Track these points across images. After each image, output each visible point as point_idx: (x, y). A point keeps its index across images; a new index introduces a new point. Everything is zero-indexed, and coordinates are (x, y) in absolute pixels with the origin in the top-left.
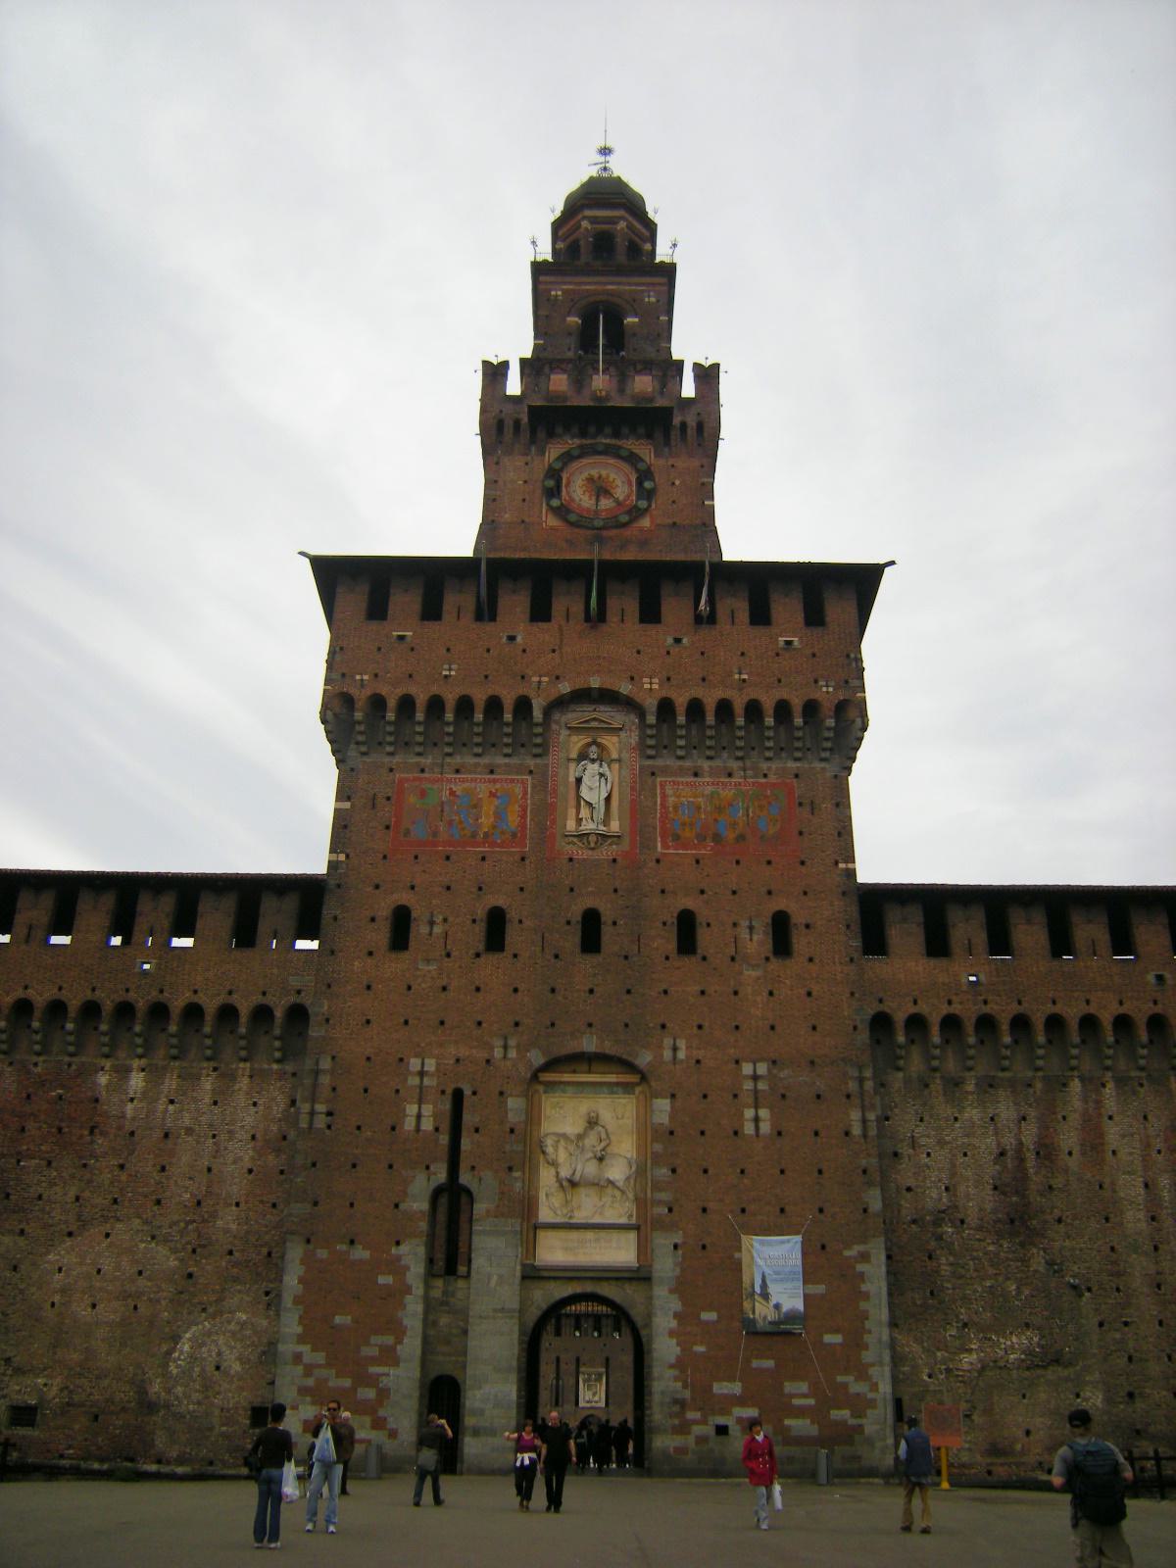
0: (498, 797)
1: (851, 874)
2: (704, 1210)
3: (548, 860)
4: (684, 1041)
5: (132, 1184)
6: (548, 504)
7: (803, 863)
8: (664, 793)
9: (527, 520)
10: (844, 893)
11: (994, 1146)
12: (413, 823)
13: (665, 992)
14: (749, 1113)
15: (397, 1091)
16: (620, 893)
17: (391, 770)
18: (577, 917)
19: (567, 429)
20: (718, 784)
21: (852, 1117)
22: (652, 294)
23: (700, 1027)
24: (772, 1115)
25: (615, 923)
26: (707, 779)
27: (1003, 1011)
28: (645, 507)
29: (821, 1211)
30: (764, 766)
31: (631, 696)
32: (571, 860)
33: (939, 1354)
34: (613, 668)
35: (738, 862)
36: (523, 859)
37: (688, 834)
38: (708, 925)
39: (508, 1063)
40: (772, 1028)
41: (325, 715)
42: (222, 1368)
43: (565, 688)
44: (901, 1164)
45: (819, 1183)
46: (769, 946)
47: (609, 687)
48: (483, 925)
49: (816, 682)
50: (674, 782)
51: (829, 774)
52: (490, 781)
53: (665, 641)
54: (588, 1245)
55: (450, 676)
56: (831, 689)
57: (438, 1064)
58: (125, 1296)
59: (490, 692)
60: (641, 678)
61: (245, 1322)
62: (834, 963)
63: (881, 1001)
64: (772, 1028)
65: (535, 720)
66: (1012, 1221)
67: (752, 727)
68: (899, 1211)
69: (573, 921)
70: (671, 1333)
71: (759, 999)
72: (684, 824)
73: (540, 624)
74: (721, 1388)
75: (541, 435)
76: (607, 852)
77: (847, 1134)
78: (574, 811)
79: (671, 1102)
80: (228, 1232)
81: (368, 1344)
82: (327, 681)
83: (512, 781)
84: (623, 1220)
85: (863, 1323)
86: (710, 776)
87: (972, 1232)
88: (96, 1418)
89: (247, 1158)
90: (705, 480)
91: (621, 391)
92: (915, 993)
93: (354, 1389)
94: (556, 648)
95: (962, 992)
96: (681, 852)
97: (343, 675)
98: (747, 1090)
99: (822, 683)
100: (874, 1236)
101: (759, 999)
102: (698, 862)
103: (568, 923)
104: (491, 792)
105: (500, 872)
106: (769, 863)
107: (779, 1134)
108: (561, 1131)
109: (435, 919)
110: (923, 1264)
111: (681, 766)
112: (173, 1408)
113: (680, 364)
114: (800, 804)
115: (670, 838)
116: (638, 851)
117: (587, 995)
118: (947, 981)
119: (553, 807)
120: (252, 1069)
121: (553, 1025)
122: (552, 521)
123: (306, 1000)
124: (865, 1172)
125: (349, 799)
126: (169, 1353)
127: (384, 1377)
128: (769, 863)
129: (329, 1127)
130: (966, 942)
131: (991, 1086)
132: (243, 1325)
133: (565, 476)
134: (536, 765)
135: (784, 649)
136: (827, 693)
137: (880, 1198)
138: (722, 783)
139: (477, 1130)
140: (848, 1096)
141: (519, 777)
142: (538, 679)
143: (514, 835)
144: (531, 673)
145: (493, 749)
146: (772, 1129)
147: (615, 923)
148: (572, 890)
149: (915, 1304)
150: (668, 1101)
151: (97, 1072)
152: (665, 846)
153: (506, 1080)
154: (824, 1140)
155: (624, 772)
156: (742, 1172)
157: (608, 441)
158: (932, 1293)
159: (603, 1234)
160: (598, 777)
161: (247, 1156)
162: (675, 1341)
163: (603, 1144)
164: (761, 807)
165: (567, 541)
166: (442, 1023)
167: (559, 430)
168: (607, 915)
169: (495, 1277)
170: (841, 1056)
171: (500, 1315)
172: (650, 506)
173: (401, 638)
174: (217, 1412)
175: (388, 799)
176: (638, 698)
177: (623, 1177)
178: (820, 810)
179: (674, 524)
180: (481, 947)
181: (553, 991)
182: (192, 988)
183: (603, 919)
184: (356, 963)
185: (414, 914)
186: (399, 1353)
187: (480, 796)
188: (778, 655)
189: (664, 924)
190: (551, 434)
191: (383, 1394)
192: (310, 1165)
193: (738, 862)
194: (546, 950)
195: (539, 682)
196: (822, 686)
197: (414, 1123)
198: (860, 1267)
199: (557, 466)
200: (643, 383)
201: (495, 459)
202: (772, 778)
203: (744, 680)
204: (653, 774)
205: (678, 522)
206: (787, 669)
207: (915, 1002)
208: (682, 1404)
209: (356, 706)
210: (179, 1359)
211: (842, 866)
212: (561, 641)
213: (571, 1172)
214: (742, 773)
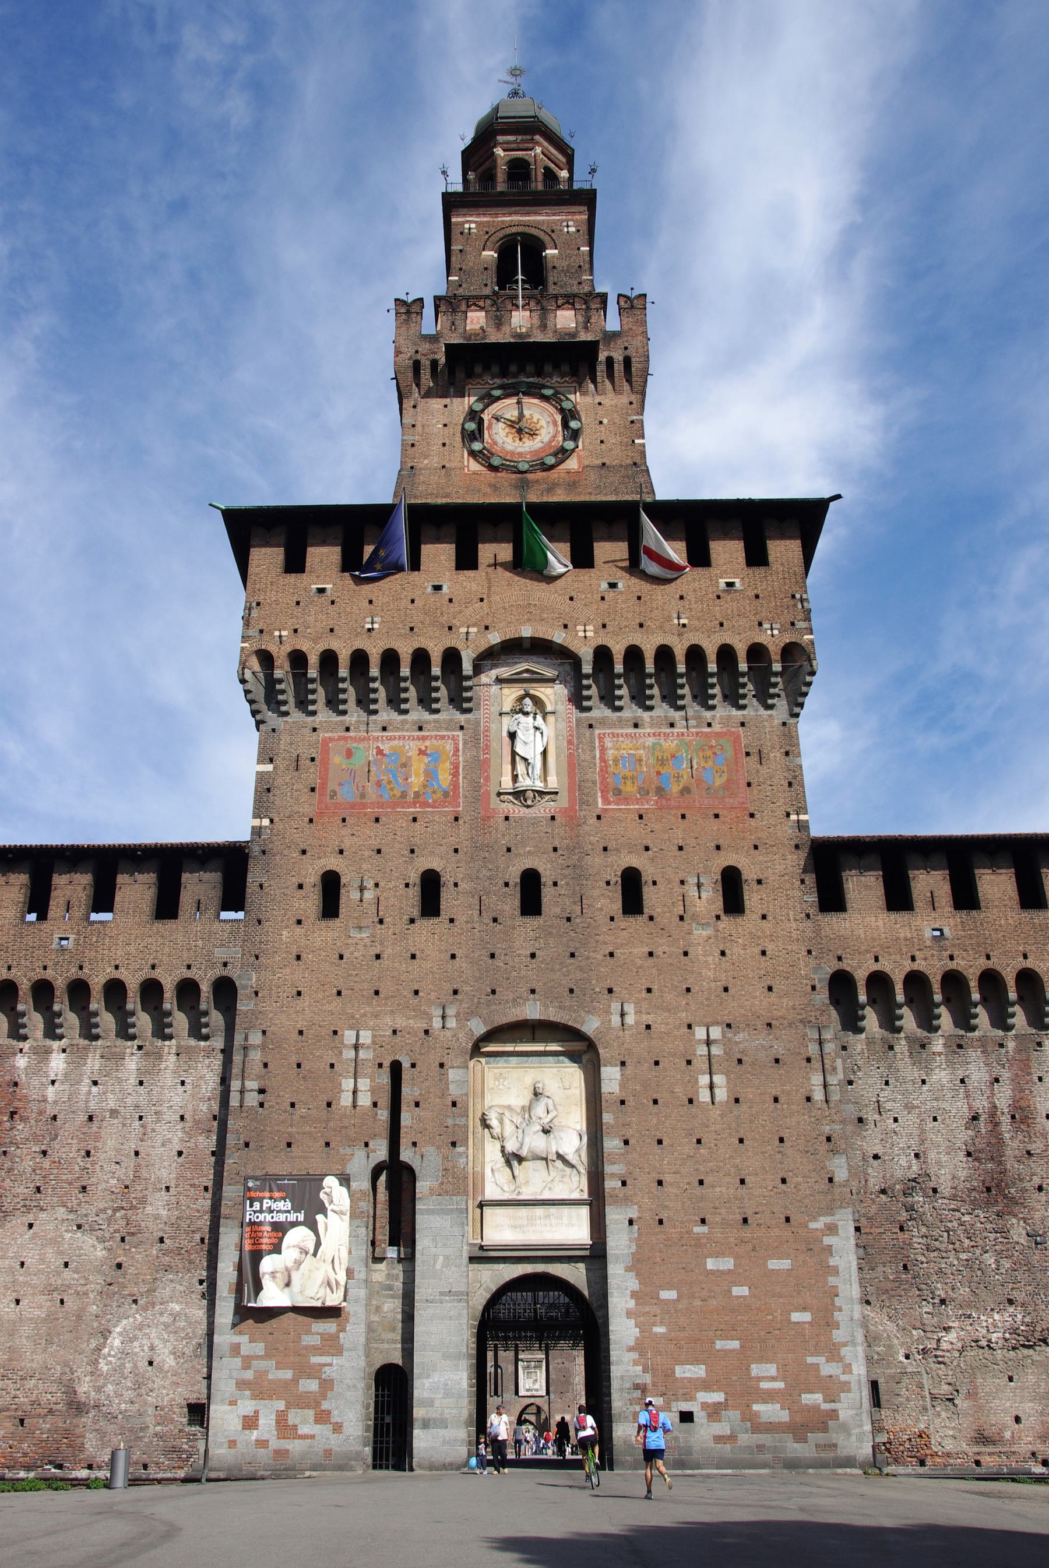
1: (802, 826)
2: (660, 1183)
3: (484, 820)
4: (632, 1005)
5: (55, 1171)
7: (752, 815)
8: (603, 746)
9: (447, 465)
10: (797, 847)
11: (966, 1110)
12: (340, 784)
13: (611, 955)
14: (704, 1080)
15: (332, 1066)
16: (560, 852)
17: (315, 730)
18: (515, 879)
19: (487, 368)
20: (659, 735)
21: (813, 1082)
22: (571, 223)
23: (649, 990)
24: (728, 1083)
25: (555, 884)
26: (648, 730)
27: (971, 966)
28: (572, 447)
29: (784, 1181)
30: (708, 715)
31: (565, 645)
32: (507, 818)
33: (914, 1332)
34: (545, 616)
35: (683, 816)
36: (456, 819)
37: (630, 788)
38: (654, 883)
39: (448, 1034)
40: (726, 990)
41: (243, 674)
42: (155, 1364)
43: (495, 638)
44: (867, 1130)
45: (779, 1152)
46: (720, 903)
47: (541, 636)
48: (418, 889)
49: (760, 624)
50: (613, 734)
51: (777, 722)
52: (418, 738)
53: (599, 586)
54: (538, 1221)
55: (373, 629)
56: (776, 632)
57: (374, 1036)
58: (50, 1290)
59: (416, 646)
60: (576, 626)
61: (178, 1314)
62: (789, 920)
63: (840, 959)
64: (726, 990)
65: (465, 673)
66: (989, 1190)
67: (694, 674)
68: (866, 1181)
69: (511, 883)
70: (629, 1314)
71: (710, 959)
72: (625, 778)
73: (465, 572)
74: (687, 1371)
75: (460, 375)
76: (544, 808)
77: (808, 1099)
78: (509, 767)
79: (621, 1070)
80: (156, 1219)
81: (309, 1332)
82: (244, 639)
83: (443, 737)
84: (576, 1195)
85: (834, 1301)
86: (651, 727)
87: (945, 1201)
88: (22, 1421)
89: (176, 1140)
90: (635, 418)
91: (543, 327)
92: (876, 949)
93: (295, 1381)
94: (485, 597)
95: (926, 947)
96: (623, 807)
97: (261, 631)
98: (701, 1056)
99: (766, 626)
100: (841, 1207)
101: (710, 959)
102: (641, 817)
103: (507, 884)
104: (420, 750)
106: (717, 816)
107: (737, 1101)
108: (506, 1103)
109: (365, 884)
110: (895, 1236)
111: (619, 717)
112: (104, 1408)
113: (603, 298)
114: (748, 754)
117: (529, 959)
118: (909, 935)
119: (487, 762)
120: (178, 1047)
121: (494, 992)
122: (474, 466)
123: (233, 972)
124: (829, 1139)
125: (271, 760)
126: (98, 1349)
127: (327, 1368)
128: (717, 816)
129: (262, 1105)
130: (929, 894)
131: (960, 1046)
132: (176, 1316)
134: (468, 721)
136: (773, 638)
137: (845, 1165)
138: (664, 734)
139: (417, 1104)
140: (809, 1060)
143: (446, 794)
144: (458, 624)
146: (728, 1097)
147: (555, 884)
148: (509, 850)
149: (886, 1278)
150: (618, 1068)
151: (15, 1054)
153: (446, 1051)
154: (785, 1106)
155: (560, 726)
156: (699, 1141)
157: (531, 380)
158: (905, 1267)
159: (553, 1210)
160: (532, 730)
161: (176, 1138)
162: (633, 1321)
163: (550, 1116)
164: (706, 758)
165: (490, 485)
166: (377, 993)
167: (478, 369)
168: (546, 878)
169: (441, 1258)
170: (800, 1017)
171: (447, 1298)
173: (321, 591)
174: (151, 1411)
175: (313, 759)
176: (575, 646)
177: (574, 1150)
178: (768, 759)
179: (604, 464)
180: (416, 912)
181: (493, 956)
182: (113, 963)
183: (543, 880)
184: (284, 933)
185: (343, 880)
186: (342, 1341)
187: (409, 754)
188: (719, 597)
189: (608, 883)
190: (470, 375)
191: (327, 1385)
192: (242, 1146)
193: (683, 816)
194: (484, 913)
195: (467, 633)
197: (351, 1099)
198: (827, 1240)
199: (478, 407)
200: (566, 319)
201: (412, 403)
202: (717, 728)
203: (684, 625)
204: (591, 726)
205: (608, 463)
206: (729, 612)
207: (877, 959)
208: (642, 1389)
209: (275, 664)
210: (109, 1355)
211: (793, 817)
212: (489, 588)
213: (518, 1145)
214: (684, 722)
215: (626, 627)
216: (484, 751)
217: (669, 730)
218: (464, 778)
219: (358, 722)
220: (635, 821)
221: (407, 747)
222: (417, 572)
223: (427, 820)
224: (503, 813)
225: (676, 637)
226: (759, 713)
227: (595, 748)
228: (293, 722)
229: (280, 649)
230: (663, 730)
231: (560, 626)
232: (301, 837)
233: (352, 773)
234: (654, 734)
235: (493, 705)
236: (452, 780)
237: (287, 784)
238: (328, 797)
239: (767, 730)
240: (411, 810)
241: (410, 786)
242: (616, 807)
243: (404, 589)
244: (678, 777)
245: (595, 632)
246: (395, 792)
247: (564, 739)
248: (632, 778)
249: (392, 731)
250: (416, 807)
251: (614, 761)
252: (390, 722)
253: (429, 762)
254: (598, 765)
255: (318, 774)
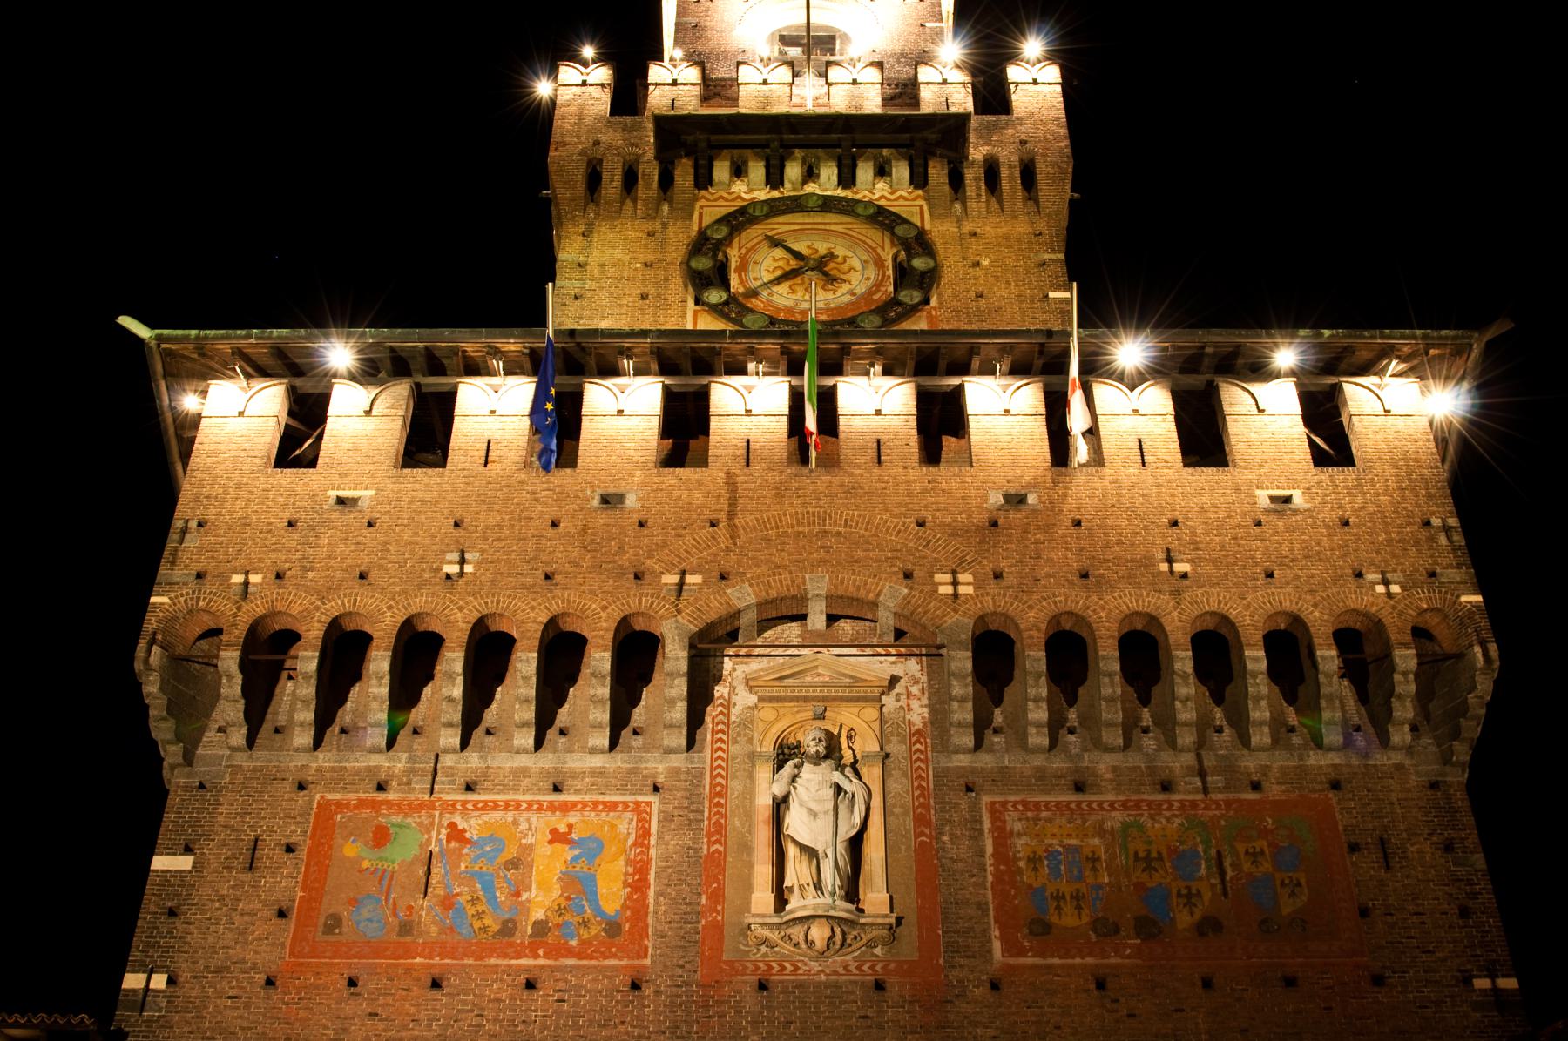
0: (571, 843)
6: (697, 302)
26: (1111, 797)
34: (860, 554)
36: (635, 986)
37: (1069, 919)
49: (1359, 575)
50: (1025, 804)
52: (552, 807)
59: (555, 608)
72: (1059, 897)
83: (611, 807)
86: (1117, 790)
96: (1056, 961)
99: (1372, 576)
102: (1101, 985)
104: (554, 832)
105: (577, 1016)
115: (1026, 931)
116: (941, 961)
125: (188, 850)
133: (734, 255)
134: (674, 772)
135: (1267, 511)
138: (1150, 804)
141: (627, 798)
142: (675, 579)
143: (613, 928)
145: (563, 739)
152: (1011, 947)
172: (927, 301)
175: (290, 849)
187: (529, 840)
196: (1374, 584)
203: (1185, 576)
206: (1285, 551)
215: (1049, 576)
216: (709, 835)
217: (1161, 797)
218: (659, 894)
219: (410, 772)
220: (1086, 991)
221: (524, 826)
222: (568, 471)
223: (562, 985)
224: (754, 972)
225: (1167, 597)
226: (1371, 763)
227: (981, 832)
228: (255, 770)
229: (239, 608)
230: (1145, 797)
231: (894, 573)
232: (241, 1017)
233: (383, 877)
234: (1125, 805)
235: (736, 742)
236: (629, 897)
237: (221, 898)
238: (321, 929)
239: (1394, 797)
240: (524, 961)
241: (525, 909)
242: (1038, 961)
243: (537, 500)
244: (1189, 896)
245: (978, 585)
246: (488, 921)
247: (906, 813)
248: (1077, 897)
249: (491, 791)
250: (536, 956)
251: (1029, 860)
252: (486, 773)
253: (575, 859)
254: (989, 869)
255: (301, 877)
